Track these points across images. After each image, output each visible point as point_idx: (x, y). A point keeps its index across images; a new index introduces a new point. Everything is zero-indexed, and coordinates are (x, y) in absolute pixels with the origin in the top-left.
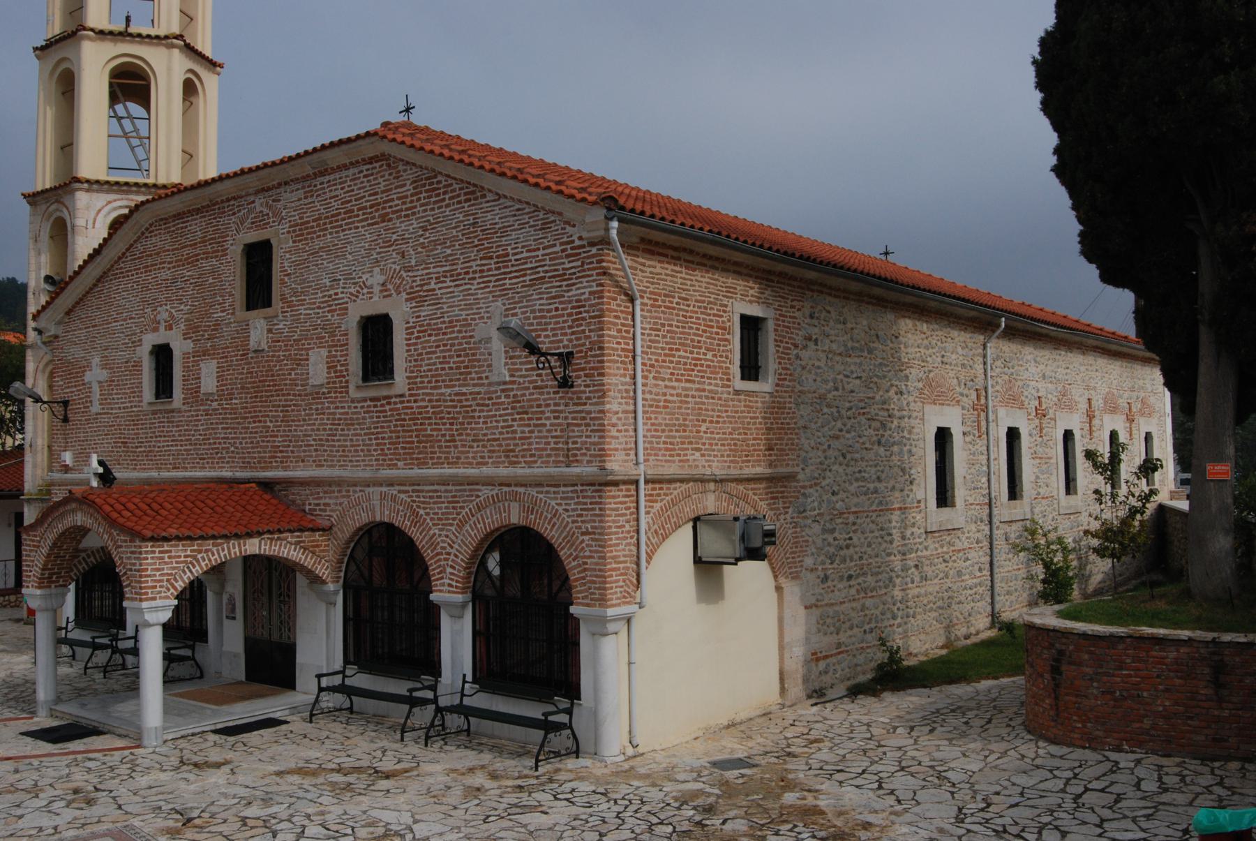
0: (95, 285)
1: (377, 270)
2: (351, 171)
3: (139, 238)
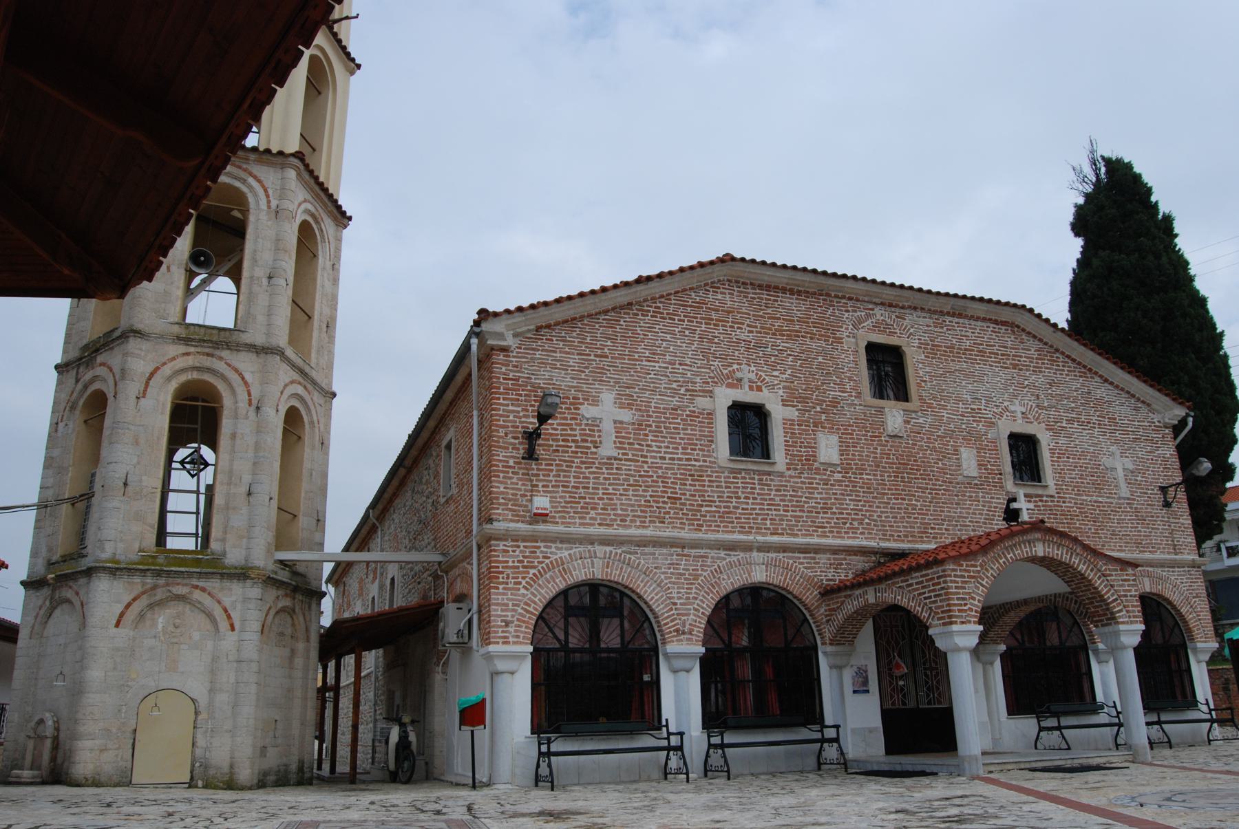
0: (606, 312)
1: (1017, 402)
2: (979, 323)
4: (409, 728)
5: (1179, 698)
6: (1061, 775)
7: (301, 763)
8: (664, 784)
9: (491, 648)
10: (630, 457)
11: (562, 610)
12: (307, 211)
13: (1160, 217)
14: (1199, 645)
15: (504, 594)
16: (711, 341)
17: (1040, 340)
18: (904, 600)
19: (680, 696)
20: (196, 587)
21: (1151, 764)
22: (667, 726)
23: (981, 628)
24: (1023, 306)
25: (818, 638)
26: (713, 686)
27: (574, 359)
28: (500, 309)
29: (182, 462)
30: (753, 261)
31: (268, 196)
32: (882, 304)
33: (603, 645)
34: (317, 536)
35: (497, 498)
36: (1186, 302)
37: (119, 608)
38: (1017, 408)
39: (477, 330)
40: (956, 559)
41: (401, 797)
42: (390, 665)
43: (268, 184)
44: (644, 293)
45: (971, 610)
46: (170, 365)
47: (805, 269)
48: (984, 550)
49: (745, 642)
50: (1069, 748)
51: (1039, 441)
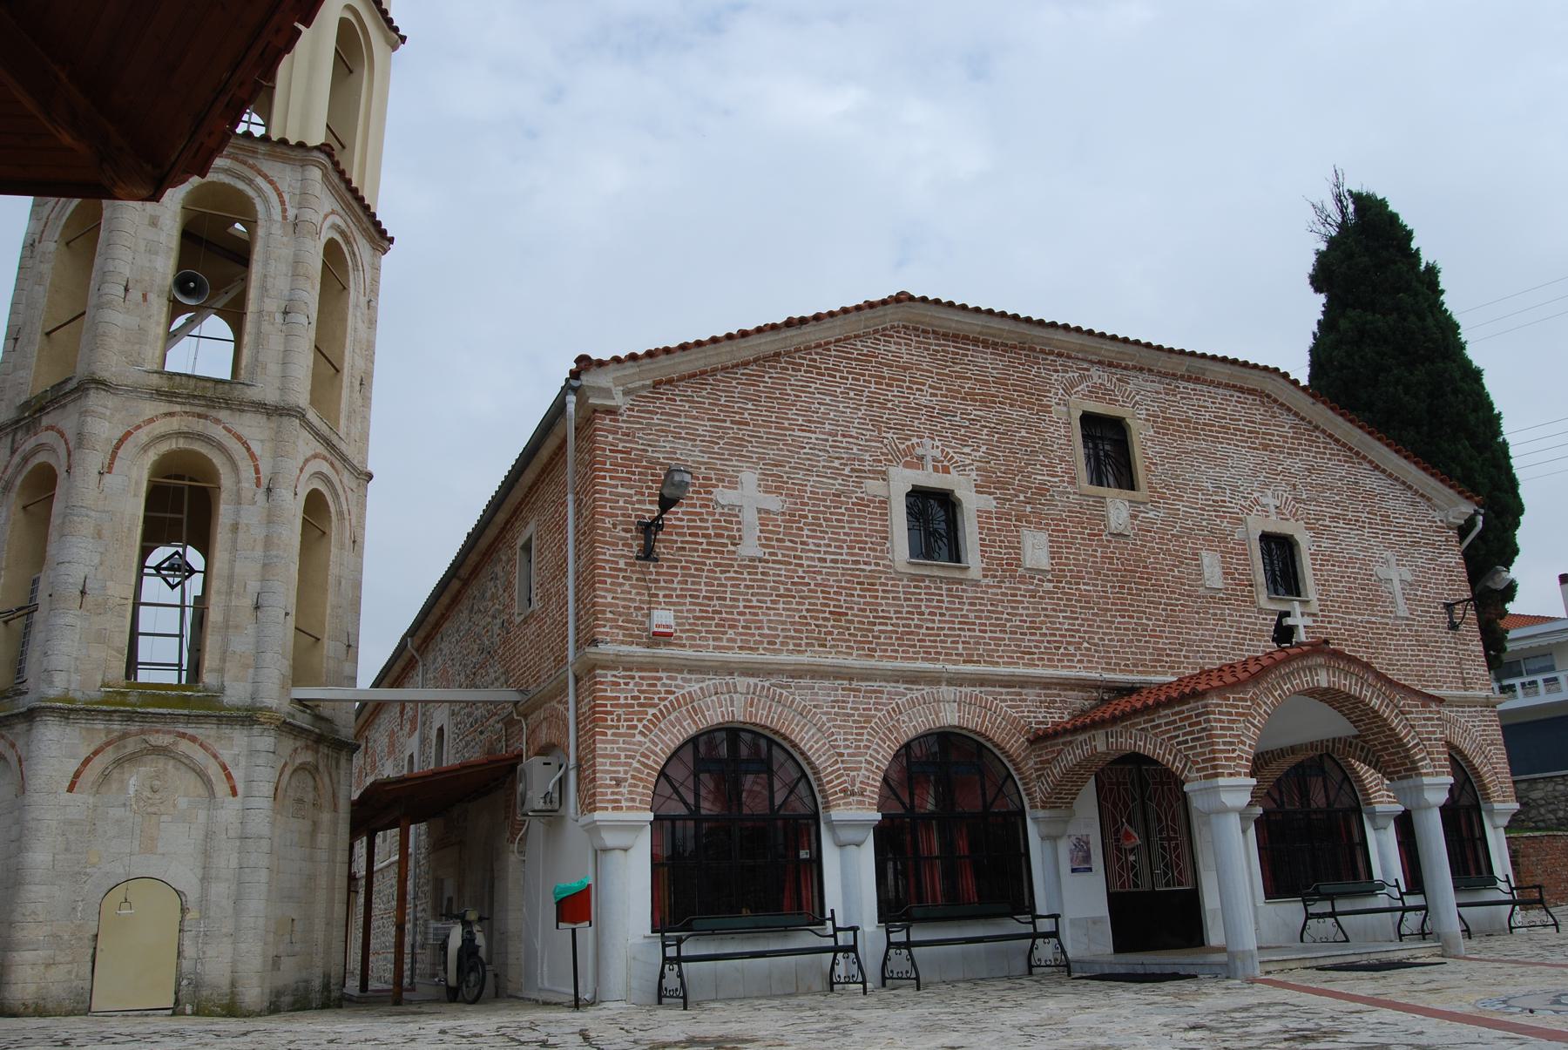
0: (746, 364)
1: (1269, 493)
2: (1220, 391)
3: (866, 334)
4: (476, 928)
5: (1473, 874)
6: (1355, 974)
7: (327, 977)
8: (832, 998)
9: (598, 815)
10: (780, 557)
11: (691, 766)
12: (335, 227)
13: (1422, 268)
14: (1497, 806)
15: (613, 742)
16: (883, 406)
17: (1296, 414)
18: (1147, 747)
19: (849, 878)
20: (183, 735)
21: (1465, 958)
22: (833, 919)
23: (1254, 781)
24: (1276, 370)
25: (1026, 800)
26: (890, 865)
27: (704, 427)
28: (607, 357)
29: (158, 568)
30: (937, 302)
31: (283, 203)
32: (1100, 363)
33: (746, 811)
34: (347, 667)
35: (604, 612)
36: (1457, 375)
37: (74, 765)
38: (1270, 501)
39: (574, 383)
40: (1223, 690)
41: (480, 1022)
42: (438, 845)
43: (283, 187)
44: (796, 340)
45: (1240, 757)
46: (146, 429)
47: (1003, 314)
48: (1255, 678)
49: (930, 807)
50: (1347, 941)
51: (1297, 543)
